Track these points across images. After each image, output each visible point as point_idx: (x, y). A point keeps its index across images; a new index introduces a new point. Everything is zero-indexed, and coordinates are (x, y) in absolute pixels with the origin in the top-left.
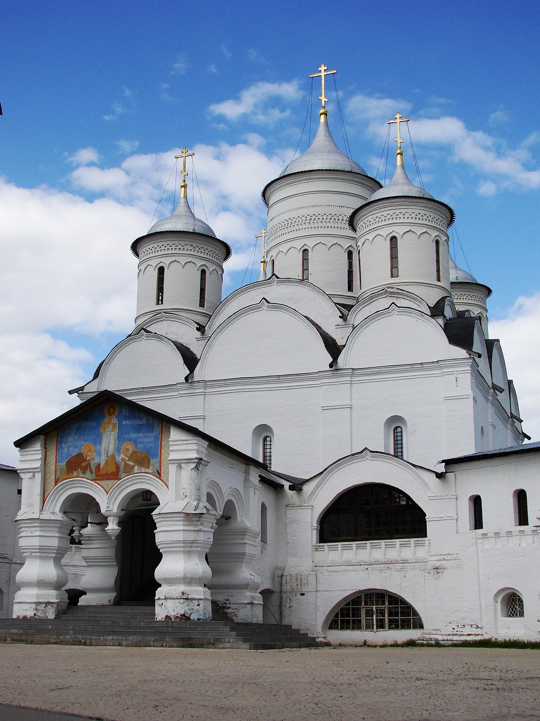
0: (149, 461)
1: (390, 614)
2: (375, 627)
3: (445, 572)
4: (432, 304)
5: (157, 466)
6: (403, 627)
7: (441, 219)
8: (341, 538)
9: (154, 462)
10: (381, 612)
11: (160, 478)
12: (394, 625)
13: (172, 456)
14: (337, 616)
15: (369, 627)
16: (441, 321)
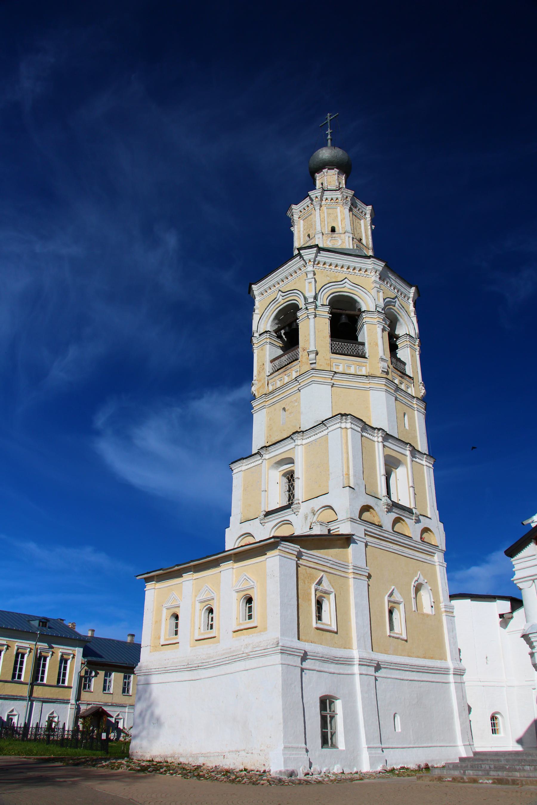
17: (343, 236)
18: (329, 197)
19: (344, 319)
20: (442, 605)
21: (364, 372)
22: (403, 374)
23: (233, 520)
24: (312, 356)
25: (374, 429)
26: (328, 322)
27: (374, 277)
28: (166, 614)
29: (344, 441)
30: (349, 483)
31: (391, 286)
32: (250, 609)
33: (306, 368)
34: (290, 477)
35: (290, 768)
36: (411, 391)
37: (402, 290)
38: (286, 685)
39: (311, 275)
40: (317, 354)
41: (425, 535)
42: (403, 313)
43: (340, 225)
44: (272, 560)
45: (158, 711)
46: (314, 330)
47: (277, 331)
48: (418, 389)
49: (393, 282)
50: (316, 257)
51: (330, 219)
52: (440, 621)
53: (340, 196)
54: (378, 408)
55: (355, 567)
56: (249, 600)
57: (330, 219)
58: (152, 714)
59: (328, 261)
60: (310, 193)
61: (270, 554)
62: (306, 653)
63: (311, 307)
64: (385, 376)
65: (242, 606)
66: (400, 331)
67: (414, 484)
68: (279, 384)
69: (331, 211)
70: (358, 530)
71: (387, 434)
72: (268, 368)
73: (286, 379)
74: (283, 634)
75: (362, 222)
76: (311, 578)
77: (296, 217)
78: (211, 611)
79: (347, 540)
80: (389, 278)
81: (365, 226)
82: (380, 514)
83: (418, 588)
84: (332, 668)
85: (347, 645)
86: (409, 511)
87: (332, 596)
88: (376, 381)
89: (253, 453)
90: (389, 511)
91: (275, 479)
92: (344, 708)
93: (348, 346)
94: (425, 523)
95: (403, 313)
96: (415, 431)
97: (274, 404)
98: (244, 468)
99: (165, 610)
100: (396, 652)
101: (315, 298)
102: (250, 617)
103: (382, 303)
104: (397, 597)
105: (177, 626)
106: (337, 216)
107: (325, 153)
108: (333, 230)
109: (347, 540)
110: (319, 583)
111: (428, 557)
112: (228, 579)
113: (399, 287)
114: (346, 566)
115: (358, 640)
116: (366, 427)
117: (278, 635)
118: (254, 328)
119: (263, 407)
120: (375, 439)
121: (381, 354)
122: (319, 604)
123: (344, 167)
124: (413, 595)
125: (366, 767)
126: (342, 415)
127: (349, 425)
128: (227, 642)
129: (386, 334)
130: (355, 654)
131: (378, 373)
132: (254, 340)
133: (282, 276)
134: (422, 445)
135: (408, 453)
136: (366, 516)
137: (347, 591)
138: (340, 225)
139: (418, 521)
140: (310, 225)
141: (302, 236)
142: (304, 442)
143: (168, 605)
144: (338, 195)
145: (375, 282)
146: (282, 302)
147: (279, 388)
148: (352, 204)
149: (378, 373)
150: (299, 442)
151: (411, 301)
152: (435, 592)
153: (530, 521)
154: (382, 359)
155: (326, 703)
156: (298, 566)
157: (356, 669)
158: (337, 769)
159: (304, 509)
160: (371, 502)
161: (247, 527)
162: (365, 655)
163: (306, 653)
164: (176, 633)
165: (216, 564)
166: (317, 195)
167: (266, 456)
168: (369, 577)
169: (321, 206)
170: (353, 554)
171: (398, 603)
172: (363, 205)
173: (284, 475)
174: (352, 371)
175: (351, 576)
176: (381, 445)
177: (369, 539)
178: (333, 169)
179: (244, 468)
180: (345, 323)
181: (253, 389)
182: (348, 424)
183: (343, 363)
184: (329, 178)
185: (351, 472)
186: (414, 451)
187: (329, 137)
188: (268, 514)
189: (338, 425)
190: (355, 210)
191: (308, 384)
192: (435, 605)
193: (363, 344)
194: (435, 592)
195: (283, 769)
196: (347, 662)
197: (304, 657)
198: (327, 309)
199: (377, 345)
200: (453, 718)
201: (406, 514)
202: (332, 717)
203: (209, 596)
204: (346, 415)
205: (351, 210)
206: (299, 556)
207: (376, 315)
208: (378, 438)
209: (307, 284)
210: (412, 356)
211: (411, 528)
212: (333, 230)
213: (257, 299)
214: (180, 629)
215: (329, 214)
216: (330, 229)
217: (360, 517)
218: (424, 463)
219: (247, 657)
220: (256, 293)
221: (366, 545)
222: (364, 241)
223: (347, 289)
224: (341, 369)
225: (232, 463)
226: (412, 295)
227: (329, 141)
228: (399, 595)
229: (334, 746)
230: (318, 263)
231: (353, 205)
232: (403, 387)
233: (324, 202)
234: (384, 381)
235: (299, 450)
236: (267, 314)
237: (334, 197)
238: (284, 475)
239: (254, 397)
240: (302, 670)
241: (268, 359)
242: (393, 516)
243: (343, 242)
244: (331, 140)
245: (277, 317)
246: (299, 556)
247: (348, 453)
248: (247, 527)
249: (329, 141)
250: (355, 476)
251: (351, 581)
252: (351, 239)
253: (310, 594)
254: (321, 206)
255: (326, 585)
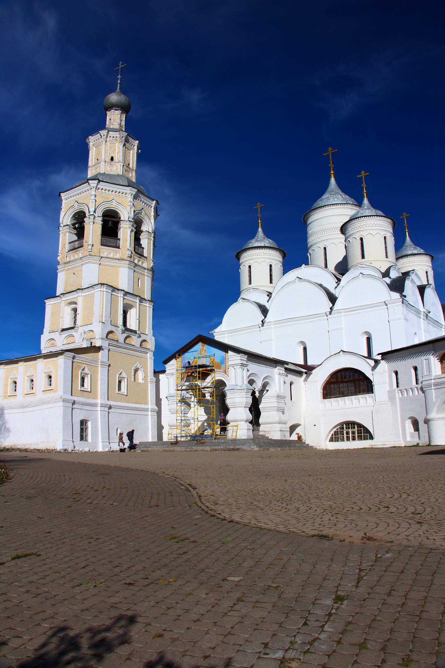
0: (221, 366)
1: (358, 433)
2: (351, 440)
3: (245, 419)
4: (383, 271)
5: (224, 368)
6: (364, 439)
7: (387, 225)
8: (332, 396)
9: (223, 366)
10: (353, 433)
11: (226, 374)
12: (360, 438)
13: (230, 363)
14: (332, 435)
15: (348, 439)
16: (388, 280)
17: (117, 164)
18: (112, 136)
19: (110, 224)
20: (149, 378)
21: (118, 256)
22: (141, 255)
23: (46, 330)
24: (90, 247)
25: (119, 290)
26: (100, 226)
27: (130, 198)
28: (10, 382)
29: (102, 298)
30: (102, 320)
31: (140, 202)
32: (51, 381)
33: (87, 253)
34: (75, 310)
35: (65, 448)
36: (145, 265)
37: (148, 203)
38: (65, 415)
39: (93, 197)
40: (93, 246)
41: (143, 343)
42: (146, 218)
43: (116, 156)
44: (61, 360)
45: (8, 425)
46: (93, 229)
47: (74, 225)
48: (148, 264)
49: (142, 199)
50: (97, 185)
51: (111, 150)
52: (147, 386)
53: (118, 136)
54: (123, 278)
55: (102, 362)
56: (50, 377)
57: (111, 150)
58: (5, 427)
59: (104, 188)
60: (101, 132)
61: (60, 357)
62: (74, 402)
63: (92, 217)
64: (129, 259)
65: (47, 380)
66: (144, 228)
67: (141, 318)
68: (72, 258)
69: (112, 145)
70: (105, 344)
71: (126, 292)
72: (67, 247)
73: (76, 257)
74: (64, 393)
75: (131, 151)
76: (79, 367)
77: (91, 145)
78: (32, 381)
79: (99, 349)
80: (140, 197)
81: (133, 154)
82: (118, 334)
83: (136, 370)
84: (87, 408)
85: (95, 398)
86: (135, 332)
87: (89, 376)
88: (124, 262)
89: (57, 295)
90: (123, 333)
91: (68, 310)
92: (92, 425)
93: (111, 241)
94: (143, 337)
95: (146, 218)
96: (144, 288)
97: (69, 269)
98: (52, 303)
99: (10, 380)
100: (120, 401)
101: (95, 212)
102: (50, 385)
103: (132, 215)
104: (124, 375)
105: (16, 387)
106: (115, 149)
107: (114, 98)
108: (112, 159)
109: (99, 349)
110: (83, 370)
111: (144, 355)
112: (40, 367)
113: (145, 201)
114: (98, 362)
115: (101, 396)
116: (114, 289)
117: (62, 393)
118: (61, 221)
119: (64, 270)
120: (119, 295)
121: (128, 246)
122: (83, 379)
123: (125, 109)
124: (133, 374)
125: (100, 449)
126: (102, 284)
127: (105, 290)
128: (40, 396)
129: (133, 233)
130: (99, 401)
131: (126, 257)
132: (61, 228)
133: (78, 192)
134: (147, 295)
135: (138, 301)
136: (110, 336)
137: (97, 373)
138: (116, 156)
139: (140, 337)
140: (99, 153)
141: (94, 159)
142: (83, 294)
143: (12, 377)
144: (117, 134)
145: (130, 202)
146: (77, 208)
147: (73, 261)
148: (126, 141)
149: (126, 257)
150: (80, 294)
151: (152, 209)
152: (146, 372)
153: (213, 332)
154: (128, 250)
155: (83, 423)
156: (73, 362)
157: (99, 408)
158: (87, 449)
159: (81, 330)
160: (113, 329)
161: (52, 336)
162: (104, 402)
163: (74, 402)
164: (15, 390)
165: (35, 359)
166: (105, 134)
167: (64, 299)
168: (109, 366)
169: (106, 142)
170: (102, 356)
171: (124, 378)
172: (133, 141)
173: (73, 310)
174: (111, 256)
175: (100, 366)
176: (122, 298)
177: (110, 347)
178: (118, 110)
179: (52, 303)
180: (110, 226)
181: (59, 258)
182: (104, 289)
183: (107, 251)
184: (115, 118)
185: (104, 315)
186: (142, 300)
187: (119, 81)
188: (63, 330)
189: (99, 289)
190: (127, 145)
191: (87, 263)
192: (145, 378)
193: (119, 240)
194: (146, 372)
195: (62, 448)
196: (95, 405)
197: (74, 403)
198: (101, 219)
199: (127, 240)
200: (148, 431)
201: (133, 334)
202: (86, 429)
203: (32, 374)
204: (104, 284)
205: (124, 145)
206: (74, 358)
207: (128, 223)
208: (121, 294)
209: (91, 202)
210: (148, 244)
211: (135, 341)
212: (112, 159)
213: (64, 202)
214: (17, 389)
215: (111, 148)
216: (110, 158)
217: (107, 337)
218: (147, 305)
219: (49, 402)
220: (63, 198)
221: (109, 350)
222: (131, 166)
223: (113, 206)
224: (105, 255)
225: (46, 299)
226: (153, 205)
227: (119, 85)
228: (125, 374)
229: (86, 440)
230: (99, 189)
231: (127, 141)
232: (140, 263)
233: (108, 139)
234: (128, 262)
235: (80, 297)
236: (68, 213)
237: (115, 136)
238: (73, 310)
239: (58, 263)
240: (73, 409)
241: (67, 242)
242: (125, 335)
243: (117, 169)
244: (120, 84)
245: (74, 216)
246: (74, 358)
247: (103, 304)
248: (52, 336)
249: (119, 85)
250: (105, 316)
251: (100, 368)
252: (122, 166)
253: (78, 375)
254: (106, 142)
255: (86, 371)
